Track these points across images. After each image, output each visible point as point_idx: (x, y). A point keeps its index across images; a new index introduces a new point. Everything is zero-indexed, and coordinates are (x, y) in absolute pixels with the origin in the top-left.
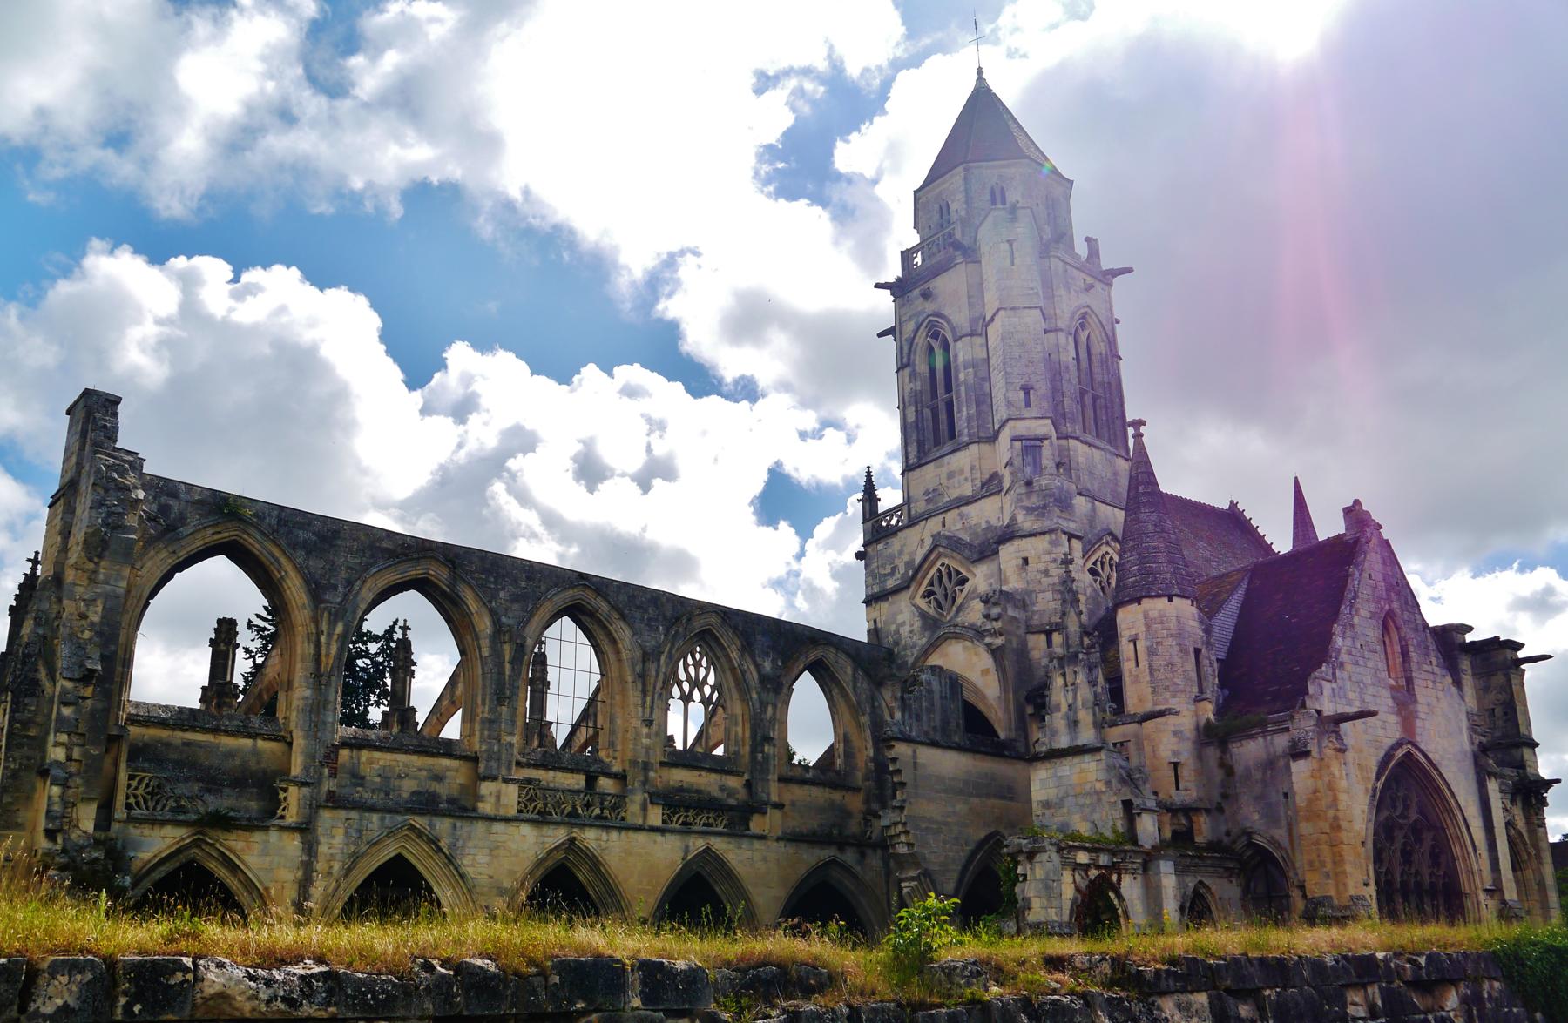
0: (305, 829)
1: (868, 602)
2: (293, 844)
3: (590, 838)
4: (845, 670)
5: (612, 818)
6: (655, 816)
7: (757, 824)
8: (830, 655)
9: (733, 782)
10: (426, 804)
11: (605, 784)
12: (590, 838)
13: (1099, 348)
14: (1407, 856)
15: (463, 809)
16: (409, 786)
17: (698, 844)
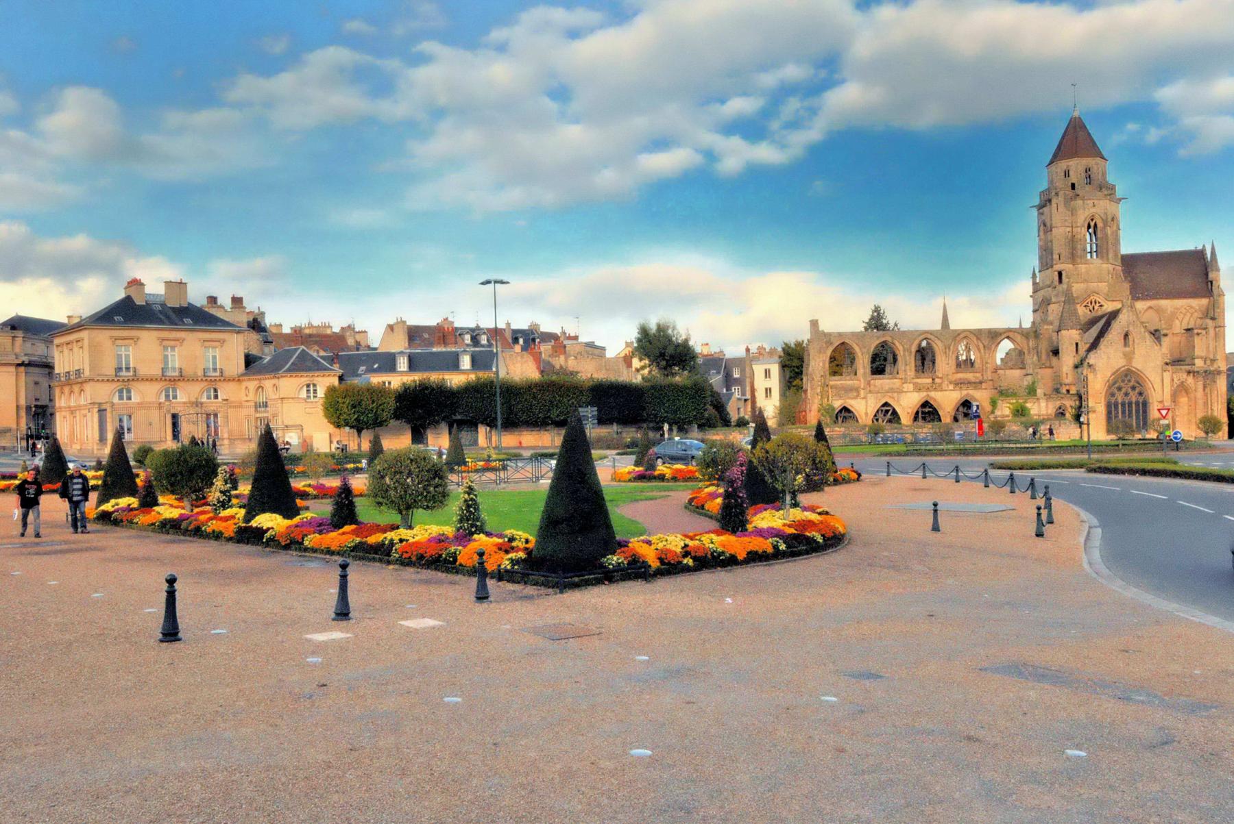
0: (865, 398)
1: (1035, 311)
2: (863, 402)
3: (933, 394)
4: (1019, 338)
5: (938, 388)
6: (951, 387)
7: (984, 386)
8: (1011, 335)
9: (978, 375)
10: (892, 390)
11: (937, 380)
12: (933, 394)
13: (1100, 225)
14: (1126, 394)
15: (900, 392)
16: (887, 388)
17: (964, 392)
